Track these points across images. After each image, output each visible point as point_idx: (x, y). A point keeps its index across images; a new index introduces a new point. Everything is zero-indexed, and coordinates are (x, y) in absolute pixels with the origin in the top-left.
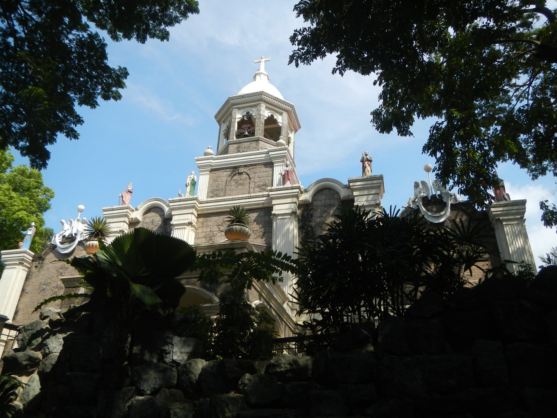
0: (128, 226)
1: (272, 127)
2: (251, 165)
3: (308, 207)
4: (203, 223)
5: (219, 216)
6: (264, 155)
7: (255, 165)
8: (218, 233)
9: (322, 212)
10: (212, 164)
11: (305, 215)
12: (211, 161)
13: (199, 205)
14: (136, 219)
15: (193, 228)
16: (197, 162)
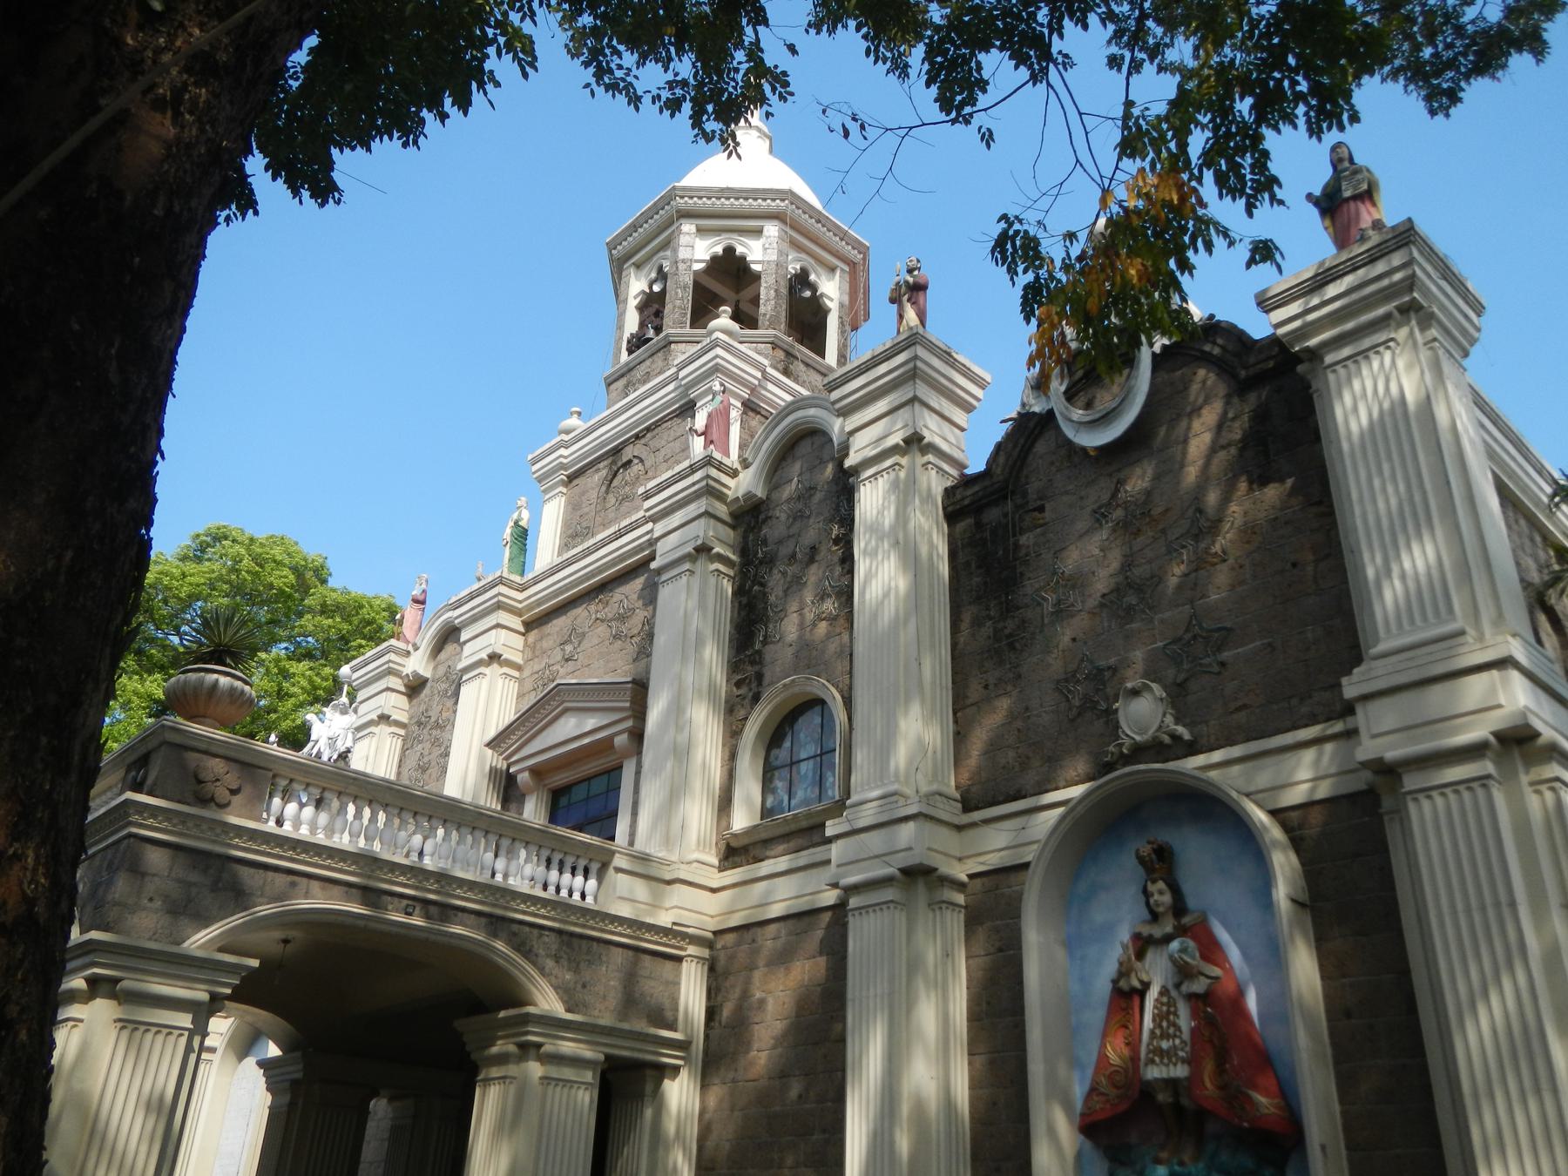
0: (405, 698)
1: (714, 281)
2: (648, 429)
3: (758, 517)
4: (533, 648)
5: (565, 613)
6: (671, 387)
7: (657, 424)
8: (562, 667)
9: (791, 520)
10: (565, 461)
11: (750, 546)
12: (563, 451)
13: (520, 596)
14: (416, 674)
15: (506, 670)
16: (535, 468)
